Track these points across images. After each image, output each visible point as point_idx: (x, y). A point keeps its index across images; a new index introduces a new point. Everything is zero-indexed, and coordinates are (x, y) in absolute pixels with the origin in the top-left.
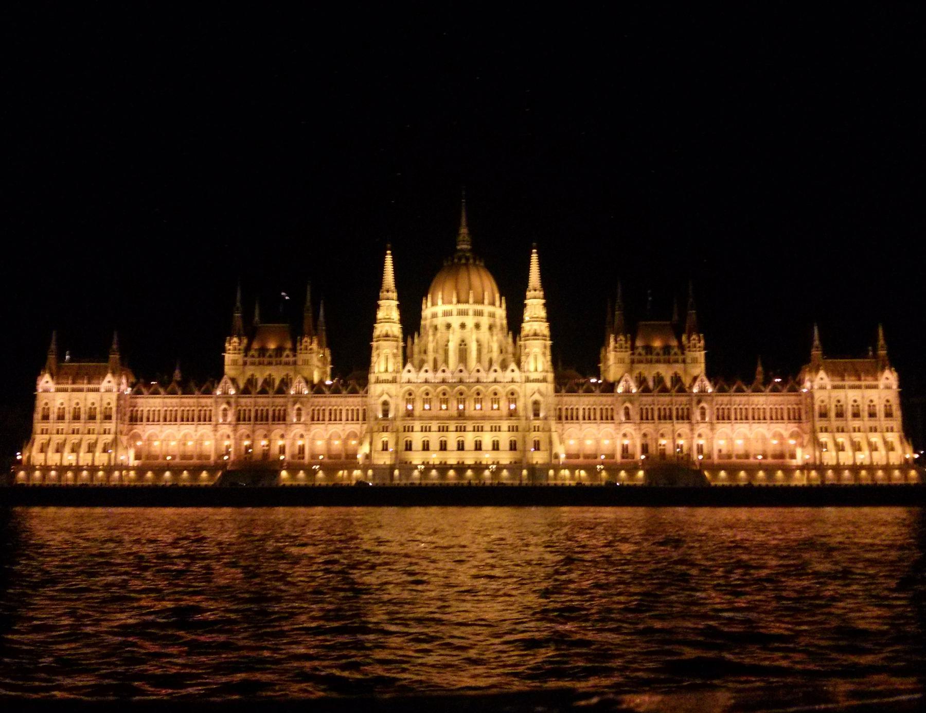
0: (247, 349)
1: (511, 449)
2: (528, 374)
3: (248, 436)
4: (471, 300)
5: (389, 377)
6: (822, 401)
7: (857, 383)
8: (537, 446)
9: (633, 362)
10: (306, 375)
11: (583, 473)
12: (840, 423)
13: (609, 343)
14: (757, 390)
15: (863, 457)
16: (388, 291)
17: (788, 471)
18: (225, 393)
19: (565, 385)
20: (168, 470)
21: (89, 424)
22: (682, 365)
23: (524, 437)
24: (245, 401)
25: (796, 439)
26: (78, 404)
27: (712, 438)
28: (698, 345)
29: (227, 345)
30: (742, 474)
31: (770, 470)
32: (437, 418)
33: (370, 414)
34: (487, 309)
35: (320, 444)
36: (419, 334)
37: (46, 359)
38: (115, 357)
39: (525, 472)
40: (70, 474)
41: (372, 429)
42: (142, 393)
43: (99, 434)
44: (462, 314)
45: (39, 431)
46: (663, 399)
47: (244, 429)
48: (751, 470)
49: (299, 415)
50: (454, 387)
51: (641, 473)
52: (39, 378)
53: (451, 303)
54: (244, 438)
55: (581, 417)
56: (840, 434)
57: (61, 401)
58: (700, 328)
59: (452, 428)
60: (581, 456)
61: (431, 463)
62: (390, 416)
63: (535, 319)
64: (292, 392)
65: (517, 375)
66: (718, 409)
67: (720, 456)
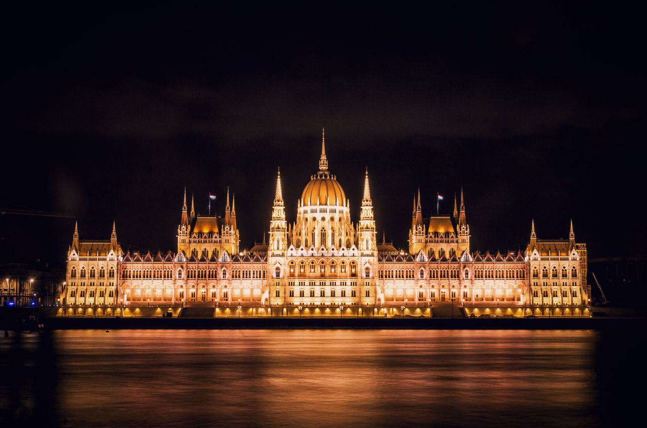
1: (352, 296)
3: (193, 286)
4: (328, 203)
5: (280, 252)
6: (535, 268)
8: (368, 294)
9: (426, 242)
11: (395, 310)
12: (545, 280)
16: (278, 201)
17: (515, 308)
19: (386, 256)
21: (103, 280)
22: (456, 244)
24: (192, 266)
26: (93, 268)
28: (466, 232)
29: (179, 230)
31: (504, 308)
32: (309, 277)
35: (237, 293)
36: (296, 224)
37: (72, 240)
38: (114, 239)
39: (360, 310)
40: (90, 310)
41: (270, 284)
43: (107, 285)
46: (444, 267)
47: (191, 282)
48: (493, 308)
49: (224, 274)
50: (319, 260)
52: (69, 252)
57: (83, 266)
58: (468, 221)
59: (317, 283)
60: (395, 299)
61: (305, 304)
62: (281, 275)
63: (367, 219)
64: (220, 260)
65: (356, 252)
66: (475, 271)
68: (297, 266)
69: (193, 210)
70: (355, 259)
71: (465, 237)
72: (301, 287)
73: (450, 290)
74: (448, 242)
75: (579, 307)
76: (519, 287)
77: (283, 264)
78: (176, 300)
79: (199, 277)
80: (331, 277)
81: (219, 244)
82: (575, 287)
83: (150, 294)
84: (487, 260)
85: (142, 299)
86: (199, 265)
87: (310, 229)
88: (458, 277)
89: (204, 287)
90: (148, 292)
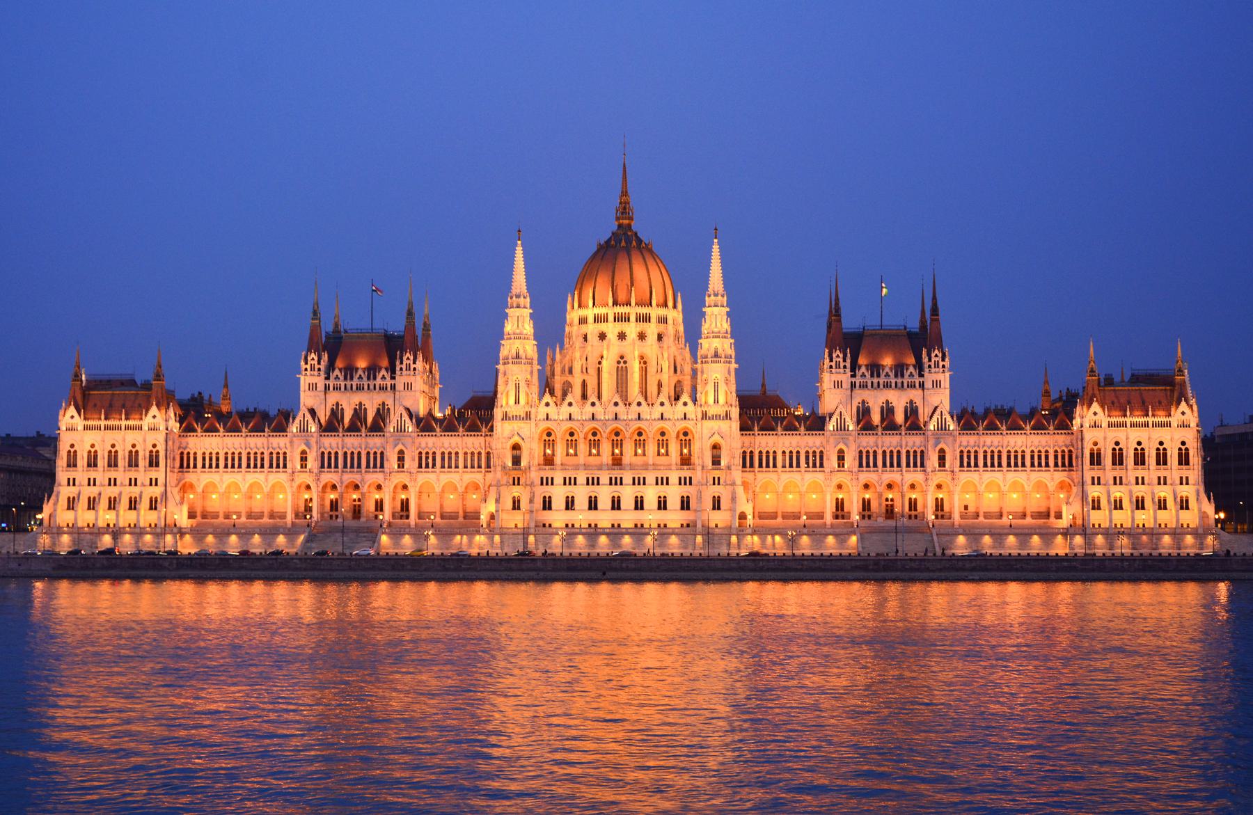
0: (331, 366)
4: (633, 303)
5: (520, 411)
8: (717, 505)
9: (853, 386)
11: (777, 538)
12: (1118, 472)
16: (518, 296)
17: (1048, 535)
18: (304, 429)
22: (920, 391)
24: (332, 443)
28: (941, 364)
31: (1024, 535)
32: (586, 467)
34: (655, 312)
36: (562, 348)
39: (699, 539)
42: (194, 430)
43: (143, 485)
47: (329, 477)
48: (998, 535)
52: (61, 413)
54: (328, 490)
59: (605, 479)
60: (780, 515)
64: (391, 428)
71: (940, 377)
72: (568, 487)
73: (903, 496)
75: (1195, 533)
76: (1062, 486)
77: (529, 434)
78: (297, 515)
80: (632, 467)
82: (1184, 487)
84: (987, 428)
85: (221, 515)
87: (593, 361)
88: (922, 465)
89: (357, 487)
90: (237, 501)
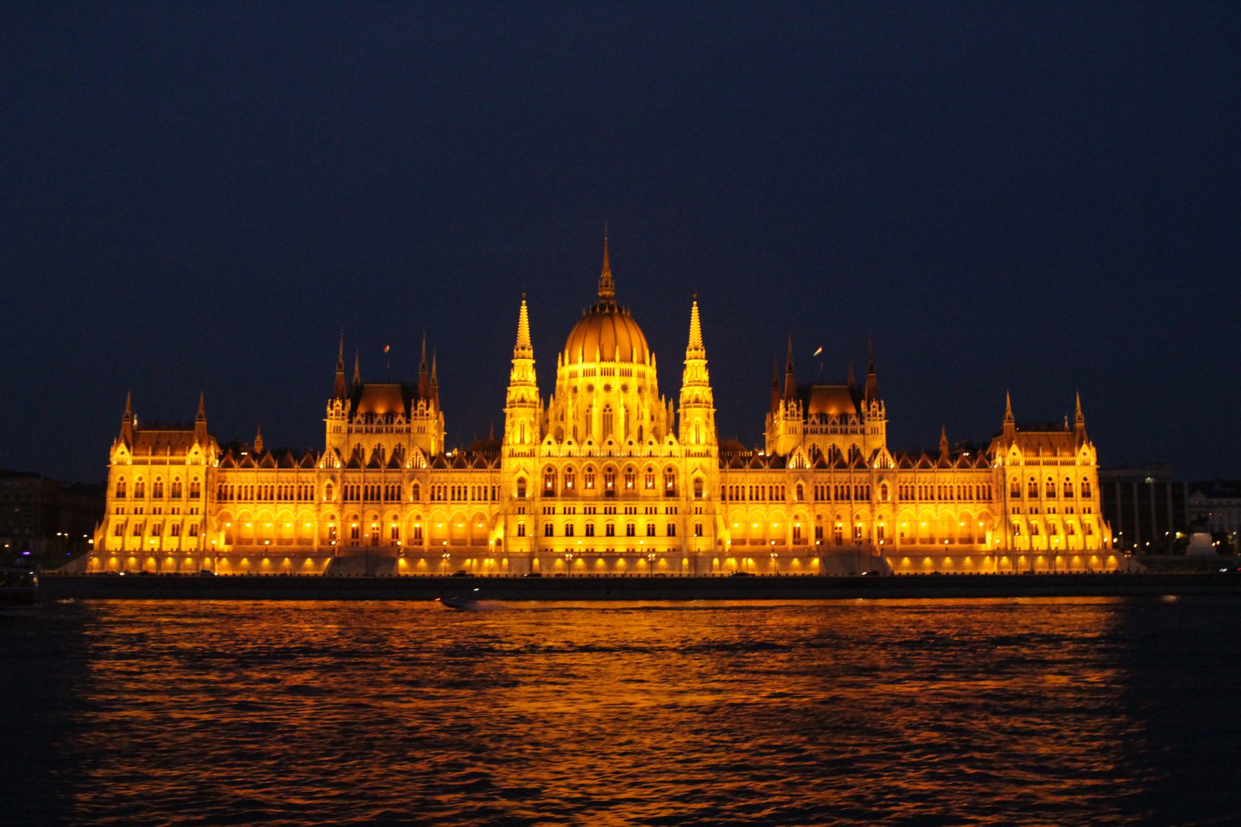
1: (669, 535)
2: (688, 447)
3: (356, 517)
4: (617, 358)
5: (525, 449)
6: (1015, 479)
7: (1053, 459)
8: (699, 531)
9: (805, 432)
10: (422, 445)
11: (750, 561)
12: (1034, 503)
13: (778, 408)
14: (943, 466)
15: (1058, 542)
16: (523, 348)
17: (977, 557)
18: (330, 466)
19: (730, 458)
20: (266, 557)
23: (684, 520)
24: (354, 477)
25: (986, 521)
26: (159, 479)
27: (894, 520)
29: (329, 408)
30: (927, 561)
31: (958, 556)
33: (502, 491)
34: (636, 368)
35: (441, 528)
37: (120, 425)
38: (201, 424)
39: (685, 561)
42: (232, 466)
43: (185, 514)
44: (606, 377)
45: (113, 510)
46: (841, 474)
47: (351, 509)
48: (937, 556)
51: (816, 562)
52: (113, 449)
53: (593, 360)
55: (747, 497)
56: (1034, 516)
59: (600, 509)
62: (528, 495)
63: (697, 383)
65: (676, 448)
67: (902, 542)
68: (559, 475)
69: (357, 375)
70: (673, 462)
74: (846, 432)
76: (980, 517)
78: (322, 542)
79: (366, 498)
81: (405, 436)
83: (272, 531)
84: (921, 467)
85: (255, 541)
86: (370, 475)
88: (868, 498)
89: (376, 518)
